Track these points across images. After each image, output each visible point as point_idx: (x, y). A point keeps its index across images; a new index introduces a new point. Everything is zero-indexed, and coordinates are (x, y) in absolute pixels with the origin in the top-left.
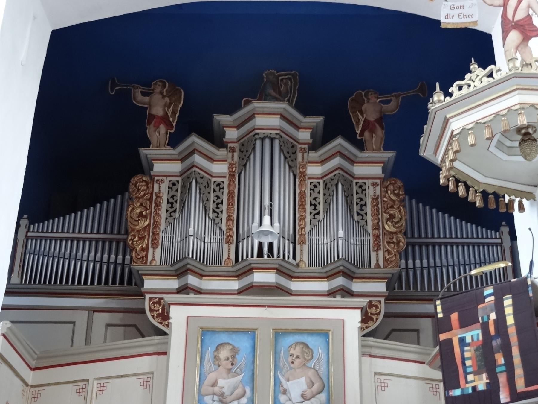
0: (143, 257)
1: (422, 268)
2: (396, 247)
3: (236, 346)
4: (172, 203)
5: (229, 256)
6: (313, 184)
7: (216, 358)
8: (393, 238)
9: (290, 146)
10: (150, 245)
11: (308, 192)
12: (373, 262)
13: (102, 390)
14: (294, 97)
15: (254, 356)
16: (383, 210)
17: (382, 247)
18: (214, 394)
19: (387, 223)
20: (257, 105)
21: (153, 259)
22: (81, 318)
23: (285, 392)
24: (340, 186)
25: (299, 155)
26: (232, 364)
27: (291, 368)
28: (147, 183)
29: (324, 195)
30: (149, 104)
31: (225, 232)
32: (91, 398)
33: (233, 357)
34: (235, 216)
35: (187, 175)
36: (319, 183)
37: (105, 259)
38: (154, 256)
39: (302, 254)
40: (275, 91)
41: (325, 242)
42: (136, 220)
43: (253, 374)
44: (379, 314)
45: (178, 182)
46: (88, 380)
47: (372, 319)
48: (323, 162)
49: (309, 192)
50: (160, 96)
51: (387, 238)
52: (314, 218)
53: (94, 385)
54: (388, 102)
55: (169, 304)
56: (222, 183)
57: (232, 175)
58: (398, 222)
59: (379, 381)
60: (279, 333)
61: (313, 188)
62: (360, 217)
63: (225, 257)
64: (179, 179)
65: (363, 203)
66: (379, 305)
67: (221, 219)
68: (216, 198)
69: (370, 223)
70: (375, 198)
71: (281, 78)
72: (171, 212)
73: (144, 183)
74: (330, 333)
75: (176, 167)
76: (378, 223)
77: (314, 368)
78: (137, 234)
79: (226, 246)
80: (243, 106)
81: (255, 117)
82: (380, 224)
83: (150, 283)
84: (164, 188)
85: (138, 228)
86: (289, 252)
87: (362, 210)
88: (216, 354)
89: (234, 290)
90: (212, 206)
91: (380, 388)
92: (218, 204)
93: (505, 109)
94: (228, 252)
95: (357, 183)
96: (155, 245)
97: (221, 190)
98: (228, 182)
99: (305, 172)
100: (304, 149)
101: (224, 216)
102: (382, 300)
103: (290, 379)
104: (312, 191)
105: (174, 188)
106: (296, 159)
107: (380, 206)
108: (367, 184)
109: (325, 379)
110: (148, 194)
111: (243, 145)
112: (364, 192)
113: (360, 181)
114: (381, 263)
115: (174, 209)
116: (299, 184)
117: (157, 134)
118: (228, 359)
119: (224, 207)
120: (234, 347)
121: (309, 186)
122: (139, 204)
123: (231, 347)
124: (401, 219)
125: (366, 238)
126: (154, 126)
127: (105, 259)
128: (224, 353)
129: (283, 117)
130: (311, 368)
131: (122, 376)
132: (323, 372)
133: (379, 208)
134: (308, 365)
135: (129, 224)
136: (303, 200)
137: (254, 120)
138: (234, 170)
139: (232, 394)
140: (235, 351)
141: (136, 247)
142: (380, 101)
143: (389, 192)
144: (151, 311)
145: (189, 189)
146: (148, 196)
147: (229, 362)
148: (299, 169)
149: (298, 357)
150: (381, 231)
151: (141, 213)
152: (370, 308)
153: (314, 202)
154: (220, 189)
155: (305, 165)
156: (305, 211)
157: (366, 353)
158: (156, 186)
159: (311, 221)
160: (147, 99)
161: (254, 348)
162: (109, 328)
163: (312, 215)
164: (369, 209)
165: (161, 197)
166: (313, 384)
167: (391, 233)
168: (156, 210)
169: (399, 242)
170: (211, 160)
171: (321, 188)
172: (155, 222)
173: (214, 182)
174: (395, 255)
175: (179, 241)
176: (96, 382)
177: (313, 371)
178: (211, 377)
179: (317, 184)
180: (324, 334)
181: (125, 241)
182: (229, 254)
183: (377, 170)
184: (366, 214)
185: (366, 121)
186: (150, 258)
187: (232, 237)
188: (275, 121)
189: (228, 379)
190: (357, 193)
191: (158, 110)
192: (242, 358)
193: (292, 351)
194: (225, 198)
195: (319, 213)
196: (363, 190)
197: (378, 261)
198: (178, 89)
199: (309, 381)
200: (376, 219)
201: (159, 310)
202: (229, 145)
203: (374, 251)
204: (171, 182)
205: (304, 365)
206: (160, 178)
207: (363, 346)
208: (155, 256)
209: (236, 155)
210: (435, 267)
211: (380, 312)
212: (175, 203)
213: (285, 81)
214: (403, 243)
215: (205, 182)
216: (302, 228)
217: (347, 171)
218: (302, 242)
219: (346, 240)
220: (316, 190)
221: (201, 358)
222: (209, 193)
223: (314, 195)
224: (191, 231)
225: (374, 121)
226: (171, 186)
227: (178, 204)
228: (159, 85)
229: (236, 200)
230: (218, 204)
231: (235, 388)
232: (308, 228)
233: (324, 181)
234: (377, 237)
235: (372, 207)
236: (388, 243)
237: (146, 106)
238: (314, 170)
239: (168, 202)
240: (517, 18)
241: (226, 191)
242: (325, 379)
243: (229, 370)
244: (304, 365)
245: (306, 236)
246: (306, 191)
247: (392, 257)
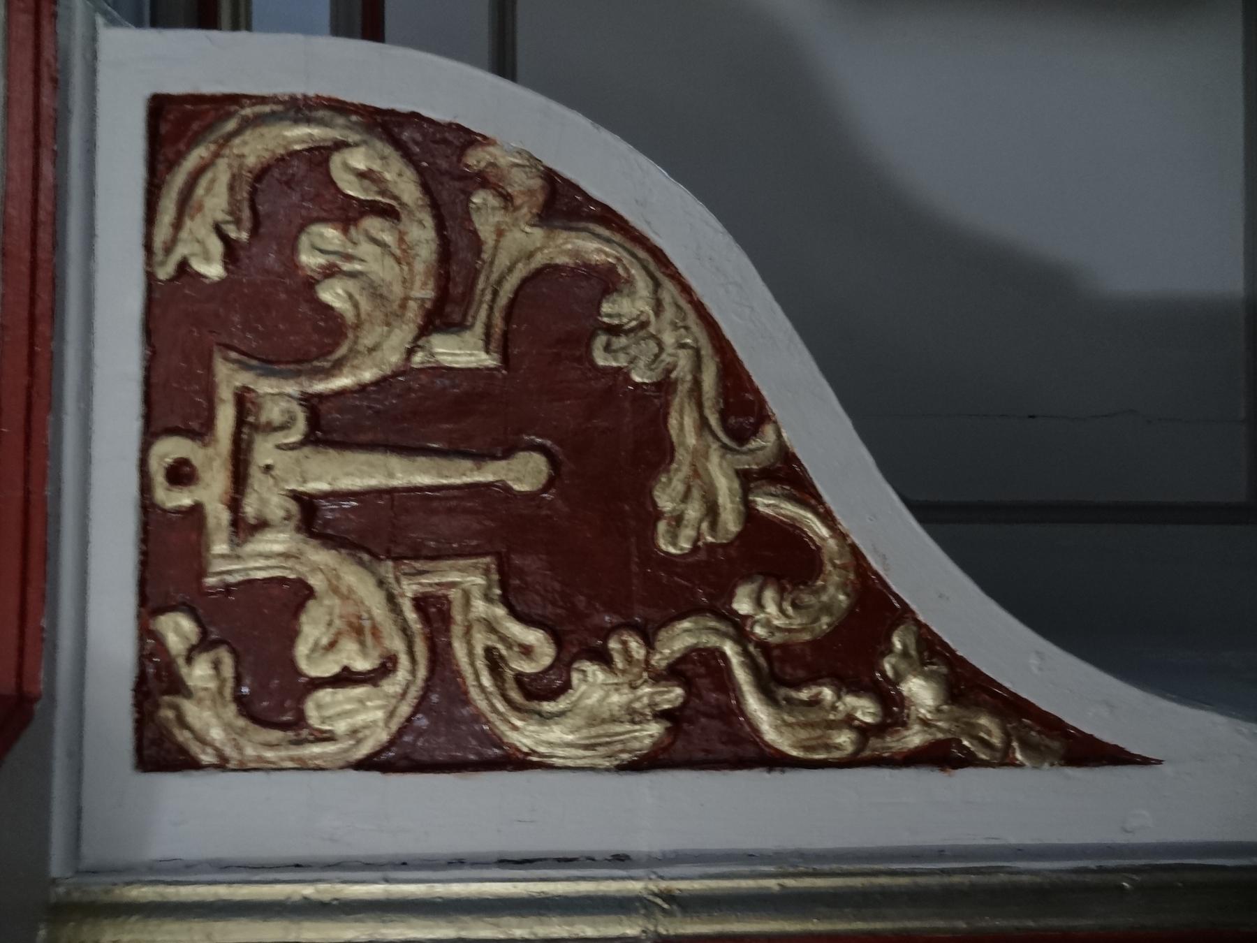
44: (441, 156)
47: (555, 315)
66: (255, 147)
152: (326, 336)
211: (385, 125)
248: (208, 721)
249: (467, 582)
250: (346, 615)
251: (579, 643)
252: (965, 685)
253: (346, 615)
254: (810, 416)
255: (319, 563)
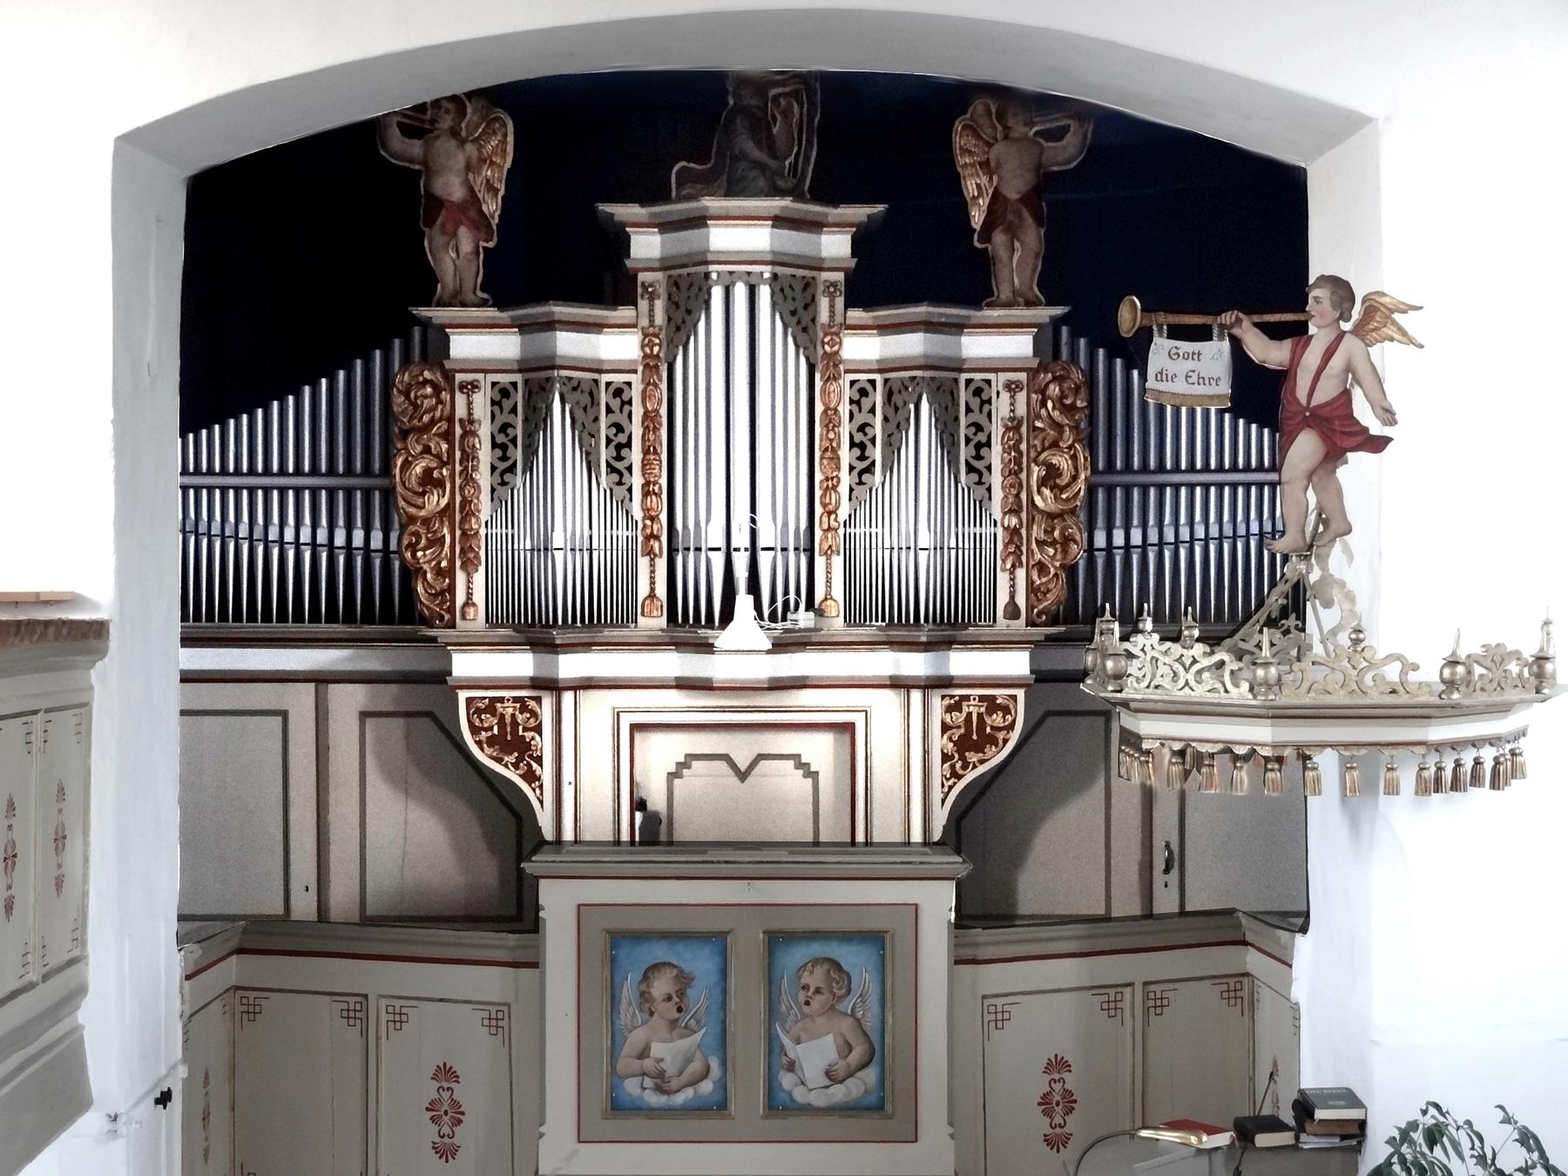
0: (442, 592)
1: (1128, 547)
2: (1059, 556)
3: (687, 970)
4: (504, 447)
5: (652, 590)
6: (857, 386)
7: (645, 997)
8: (1053, 529)
9: (798, 286)
10: (458, 563)
11: (844, 409)
12: (1003, 599)
13: (399, 1020)
14: (807, 159)
15: (724, 992)
16: (1033, 455)
17: (1024, 558)
18: (644, 1074)
19: (1039, 492)
20: (712, 203)
21: (469, 602)
22: (300, 700)
23: (791, 1067)
24: (925, 406)
25: (824, 303)
26: (680, 1010)
27: (804, 1016)
28: (437, 390)
29: (886, 419)
30: (425, 162)
31: (640, 526)
32: (378, 1038)
33: (681, 994)
34: (664, 481)
35: (536, 382)
36: (873, 382)
37: (340, 540)
38: (469, 595)
39: (828, 581)
40: (757, 142)
41: (887, 545)
42: (415, 493)
43: (724, 1031)
44: (1011, 727)
45: (514, 384)
46: (366, 996)
47: (994, 742)
48: (885, 329)
49: (848, 407)
50: (453, 143)
51: (1037, 532)
52: (861, 483)
53: (379, 1011)
54: (1057, 135)
55: (537, 878)
56: (625, 388)
57: (650, 364)
58: (1068, 485)
59: (992, 1009)
60: (777, 939)
61: (856, 397)
62: (975, 477)
63: (643, 591)
64: (518, 378)
65: (982, 437)
67: (630, 490)
68: (614, 430)
69: (998, 494)
70: (1013, 425)
71: (773, 92)
72: (504, 472)
73: (429, 390)
74: (888, 937)
75: (503, 346)
76: (1017, 496)
77: (853, 1015)
78: (422, 531)
79: (643, 562)
80: (674, 194)
81: (707, 226)
82: (1024, 496)
83: (465, 665)
84: (481, 404)
85: (423, 513)
86: (798, 593)
87: (978, 457)
88: (643, 987)
89: (668, 679)
90: (604, 454)
91: (992, 1025)
92: (619, 447)
93: (1244, 744)
94: (650, 578)
95: (969, 382)
96: (469, 565)
97: (626, 407)
98: (641, 387)
99: (837, 353)
100: (834, 284)
101: (637, 481)
102: (1020, 694)
103: (803, 1037)
104: (855, 408)
105: (507, 404)
106: (813, 320)
107: (1023, 447)
108: (993, 384)
109: (875, 1038)
110: (440, 420)
111: (676, 284)
112: (986, 408)
113: (977, 376)
114: (1021, 601)
115: (510, 462)
116: (823, 391)
117: (453, 255)
118: (669, 998)
119: (636, 455)
120: (681, 972)
121: (847, 393)
122: (419, 448)
123: (675, 972)
124: (1075, 478)
125: (987, 530)
126: (443, 233)
127: (340, 540)
128: (661, 986)
129: (779, 221)
130: (846, 1014)
131: (441, 1000)
132: (871, 1023)
133: (1021, 453)
134: (840, 1007)
135: (402, 503)
136: (831, 435)
137: (703, 230)
138: (656, 349)
139: (681, 1073)
140: (684, 981)
141: (426, 567)
142: (1037, 133)
143: (1050, 404)
144: (475, 730)
145: (545, 420)
146: (444, 425)
147: (672, 1006)
148: (823, 344)
149: (818, 991)
150: (1024, 515)
151: (428, 471)
153: (859, 437)
154: (623, 403)
155: (837, 334)
156: (838, 468)
157: (961, 960)
158: (460, 399)
159: (851, 490)
160: (415, 147)
161: (724, 972)
162: (370, 722)
163: (855, 472)
164: (996, 455)
165: (474, 434)
166: (850, 1050)
167: (1051, 516)
168: (466, 468)
169: (1067, 540)
170: (596, 327)
171: (878, 398)
172: (466, 502)
173: (608, 384)
174: (1056, 575)
175: (528, 546)
176: (383, 1003)
177: (850, 1020)
178: (636, 1038)
179: (869, 388)
180: (876, 939)
181: (388, 495)
182: (653, 583)
183: (1019, 346)
184: (989, 468)
185: (997, 196)
186: (460, 598)
187: (657, 538)
188: (757, 238)
189: (672, 1040)
190: (969, 410)
191: (451, 187)
192: (700, 996)
193: (806, 979)
194: (637, 431)
195: (869, 469)
196: (983, 403)
197: (1012, 596)
198: (497, 119)
199: (841, 1041)
200: (1012, 486)
201: (491, 728)
202: (642, 277)
203: (1003, 570)
204: (497, 388)
205: (832, 1007)
206: (469, 377)
207: (956, 944)
208: (472, 588)
209: (659, 305)
210: (1161, 544)
212: (511, 446)
213: (783, 102)
214: (1076, 542)
215: (589, 392)
216: (830, 513)
217: (943, 364)
218: (828, 553)
219: (939, 548)
220: (866, 403)
221: (613, 997)
222: (596, 419)
223: (860, 419)
224: (558, 540)
225: (1019, 200)
226: (497, 398)
227: (519, 448)
228: (447, 112)
229: (665, 426)
230: (619, 447)
231: (688, 1060)
232: (844, 513)
233: (886, 381)
234: (1014, 533)
235: (1004, 451)
236: (1040, 543)
237: (417, 167)
238: (862, 348)
239: (494, 445)
240: (1320, 397)
241: (637, 411)
242: (875, 1038)
243: (673, 1024)
244: (832, 1007)
245: (841, 531)
246: (840, 408)
247: (1049, 581)
248: (947, 702)
249: (962, 731)
250: (960, 718)
251: (955, 743)
252: (951, 788)
253: (960, 718)
254: (982, 769)
255: (964, 714)
